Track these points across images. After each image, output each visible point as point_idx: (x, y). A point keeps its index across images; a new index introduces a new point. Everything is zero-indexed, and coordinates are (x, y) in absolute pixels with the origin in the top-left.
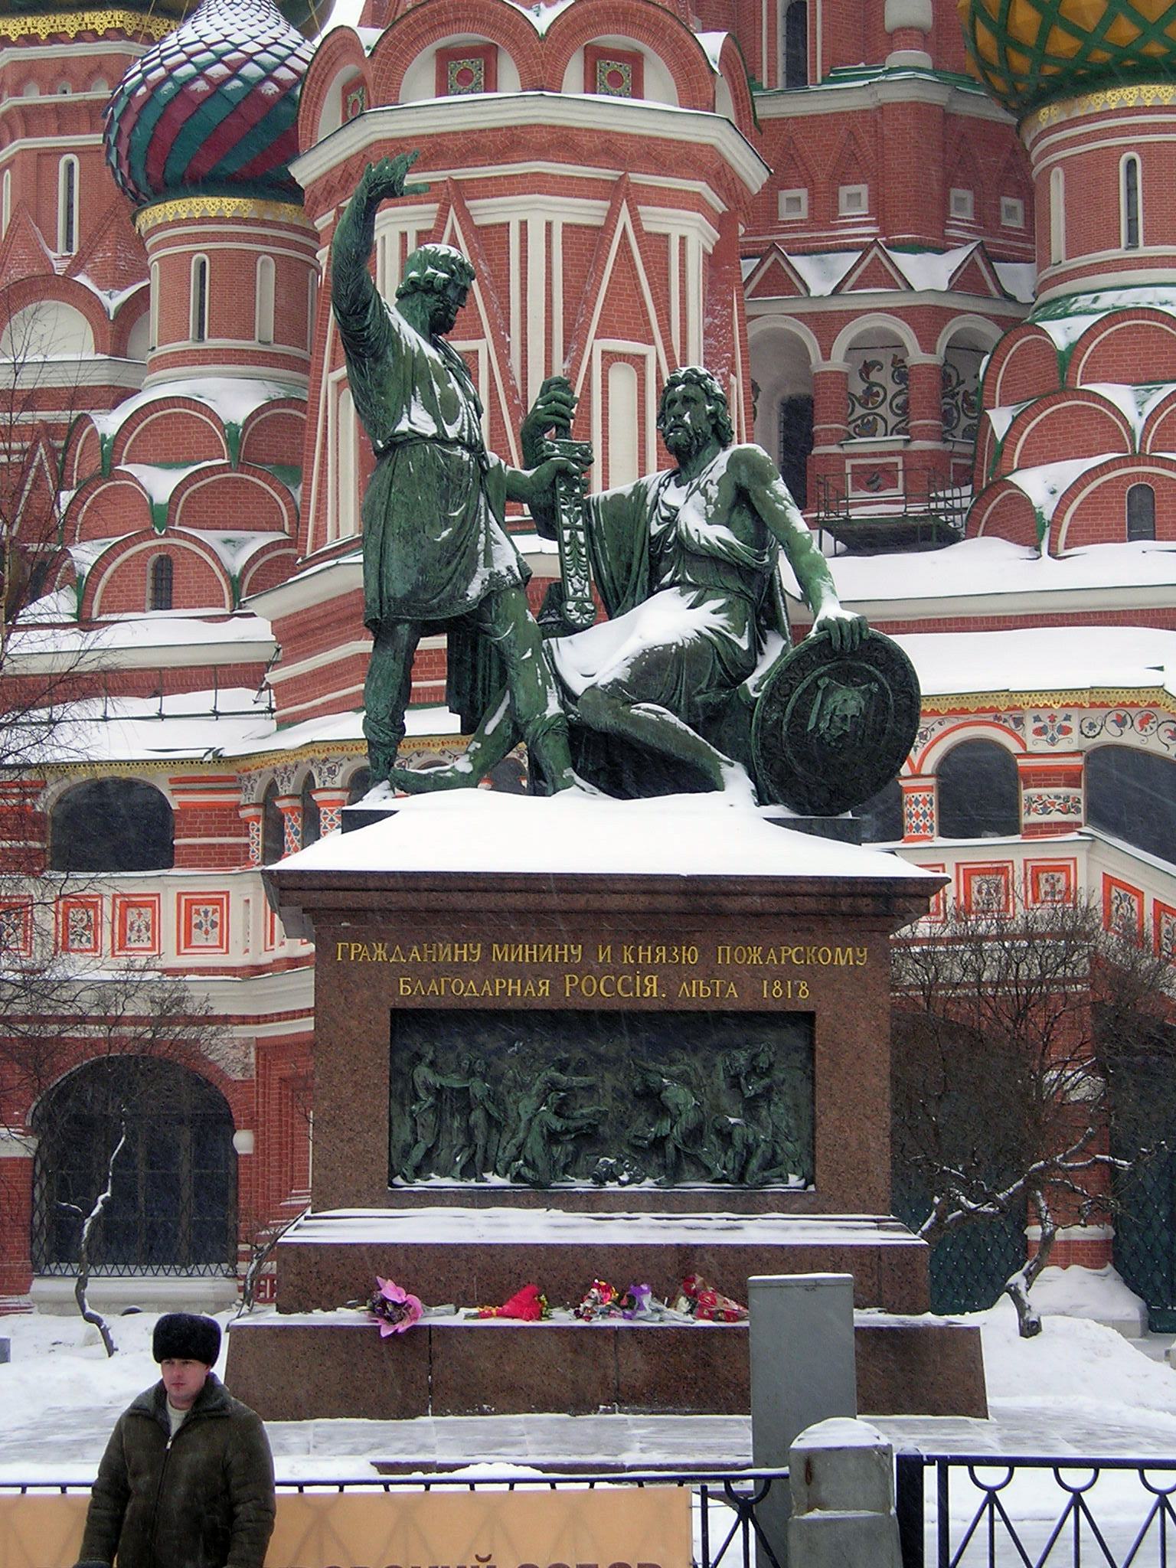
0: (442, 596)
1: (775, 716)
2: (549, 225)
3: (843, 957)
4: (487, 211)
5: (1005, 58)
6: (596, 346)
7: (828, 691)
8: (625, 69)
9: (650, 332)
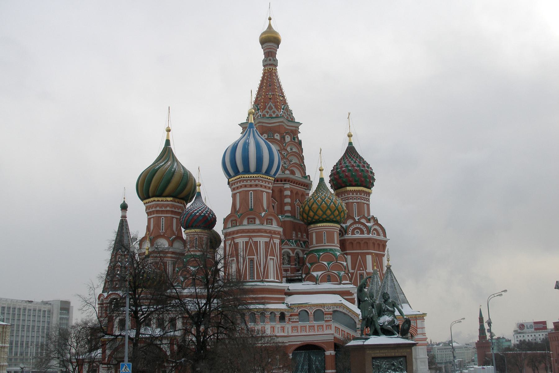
3: (408, 350)
4: (255, 239)
6: (269, 257)
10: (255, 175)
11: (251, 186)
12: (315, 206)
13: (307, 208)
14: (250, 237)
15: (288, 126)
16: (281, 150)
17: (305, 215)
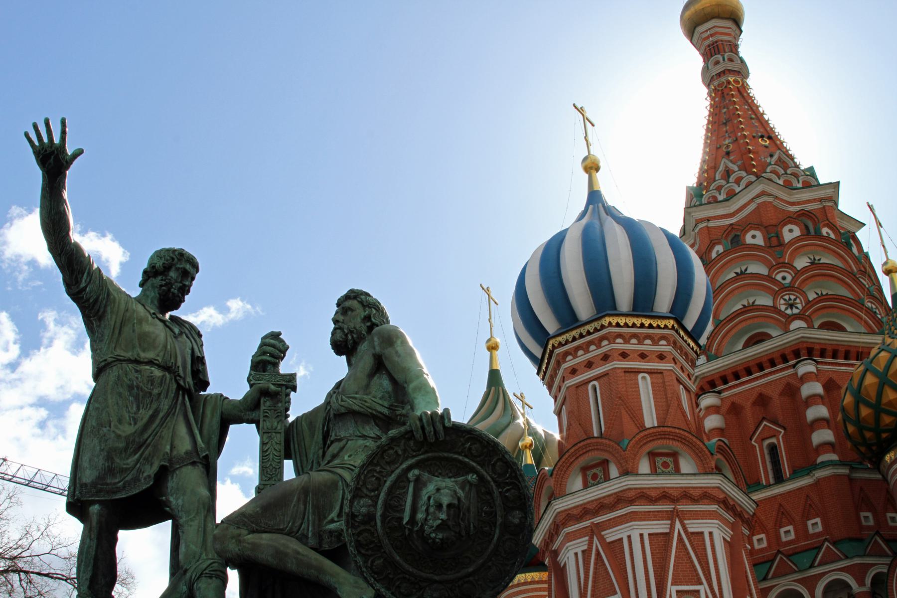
0: (127, 479)
1: (364, 510)
2: (641, 535)
4: (611, 535)
5: (863, 437)
7: (419, 484)
8: (669, 460)
9: (699, 579)
10: (591, 328)
11: (589, 365)
12: (870, 379)
13: (848, 399)
14: (595, 531)
15: (793, 204)
16: (771, 268)
17: (851, 429)
